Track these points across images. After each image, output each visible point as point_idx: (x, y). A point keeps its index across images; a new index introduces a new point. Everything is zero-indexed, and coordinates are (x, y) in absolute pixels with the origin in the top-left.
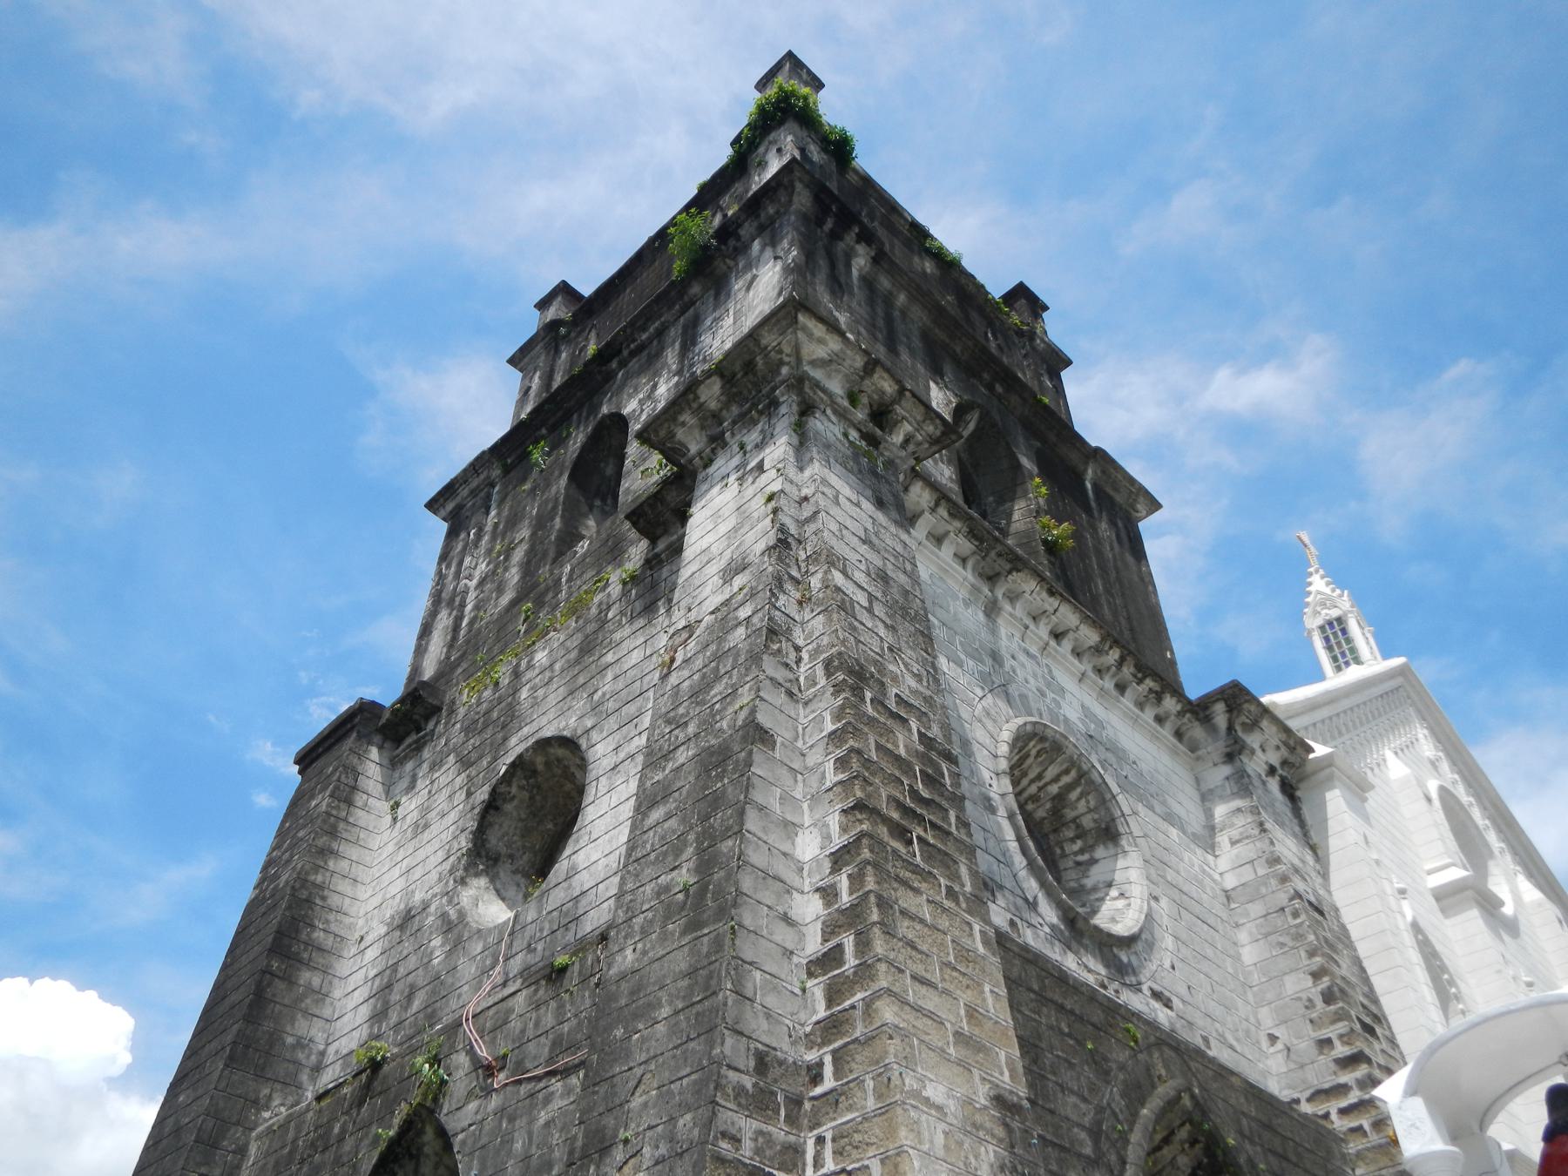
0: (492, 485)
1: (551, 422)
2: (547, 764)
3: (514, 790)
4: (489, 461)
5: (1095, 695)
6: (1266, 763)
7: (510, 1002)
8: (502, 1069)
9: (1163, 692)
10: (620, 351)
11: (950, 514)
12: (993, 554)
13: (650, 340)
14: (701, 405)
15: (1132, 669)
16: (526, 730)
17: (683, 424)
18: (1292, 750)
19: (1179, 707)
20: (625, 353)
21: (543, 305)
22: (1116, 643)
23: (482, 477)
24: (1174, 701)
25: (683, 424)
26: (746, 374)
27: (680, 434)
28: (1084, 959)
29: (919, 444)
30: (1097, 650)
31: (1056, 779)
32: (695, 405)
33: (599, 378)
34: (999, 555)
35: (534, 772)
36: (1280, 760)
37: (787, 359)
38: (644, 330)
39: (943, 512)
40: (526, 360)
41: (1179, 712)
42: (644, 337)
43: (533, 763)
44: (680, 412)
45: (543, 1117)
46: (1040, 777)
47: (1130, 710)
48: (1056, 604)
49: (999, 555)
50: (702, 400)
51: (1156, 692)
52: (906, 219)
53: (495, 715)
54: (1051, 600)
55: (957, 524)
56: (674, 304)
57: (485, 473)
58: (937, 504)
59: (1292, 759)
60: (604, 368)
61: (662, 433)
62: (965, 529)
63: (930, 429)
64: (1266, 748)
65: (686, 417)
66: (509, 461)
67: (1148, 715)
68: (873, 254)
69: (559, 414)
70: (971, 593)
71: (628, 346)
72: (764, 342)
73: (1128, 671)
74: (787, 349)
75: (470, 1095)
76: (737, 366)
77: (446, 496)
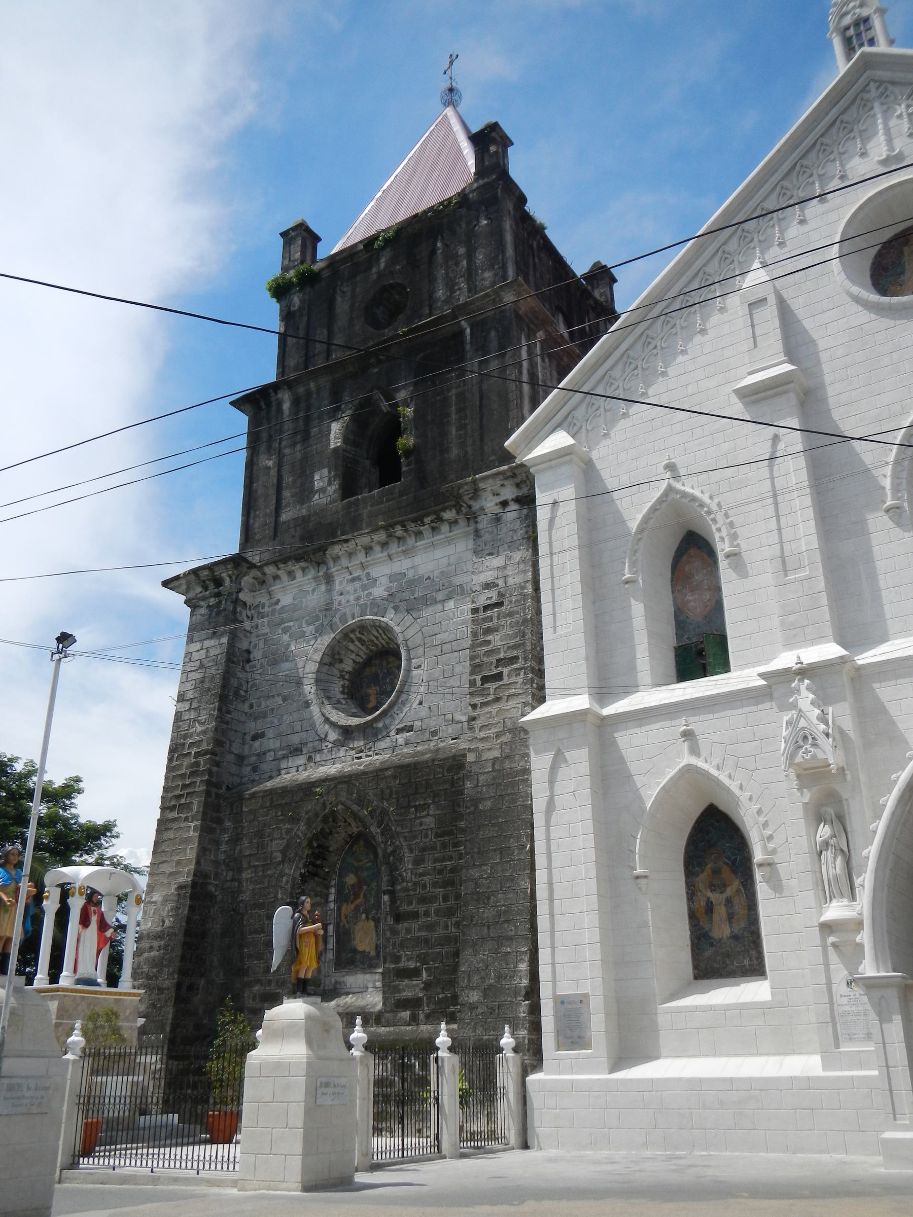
5: (403, 558)
6: (496, 504)
9: (438, 515)
11: (284, 563)
12: (311, 556)
15: (413, 525)
18: (514, 476)
19: (454, 511)
22: (392, 526)
24: (448, 512)
28: (351, 746)
29: (233, 574)
30: (390, 536)
31: (380, 634)
34: (314, 554)
36: (514, 487)
39: (281, 566)
41: (458, 513)
46: (377, 638)
47: (426, 544)
48: (353, 542)
49: (314, 554)
51: (436, 519)
52: (361, 251)
54: (350, 543)
55: (290, 563)
58: (277, 566)
59: (518, 480)
62: (294, 562)
63: (229, 566)
64: (498, 492)
67: (445, 528)
68: (286, 387)
70: (316, 581)
73: (411, 526)
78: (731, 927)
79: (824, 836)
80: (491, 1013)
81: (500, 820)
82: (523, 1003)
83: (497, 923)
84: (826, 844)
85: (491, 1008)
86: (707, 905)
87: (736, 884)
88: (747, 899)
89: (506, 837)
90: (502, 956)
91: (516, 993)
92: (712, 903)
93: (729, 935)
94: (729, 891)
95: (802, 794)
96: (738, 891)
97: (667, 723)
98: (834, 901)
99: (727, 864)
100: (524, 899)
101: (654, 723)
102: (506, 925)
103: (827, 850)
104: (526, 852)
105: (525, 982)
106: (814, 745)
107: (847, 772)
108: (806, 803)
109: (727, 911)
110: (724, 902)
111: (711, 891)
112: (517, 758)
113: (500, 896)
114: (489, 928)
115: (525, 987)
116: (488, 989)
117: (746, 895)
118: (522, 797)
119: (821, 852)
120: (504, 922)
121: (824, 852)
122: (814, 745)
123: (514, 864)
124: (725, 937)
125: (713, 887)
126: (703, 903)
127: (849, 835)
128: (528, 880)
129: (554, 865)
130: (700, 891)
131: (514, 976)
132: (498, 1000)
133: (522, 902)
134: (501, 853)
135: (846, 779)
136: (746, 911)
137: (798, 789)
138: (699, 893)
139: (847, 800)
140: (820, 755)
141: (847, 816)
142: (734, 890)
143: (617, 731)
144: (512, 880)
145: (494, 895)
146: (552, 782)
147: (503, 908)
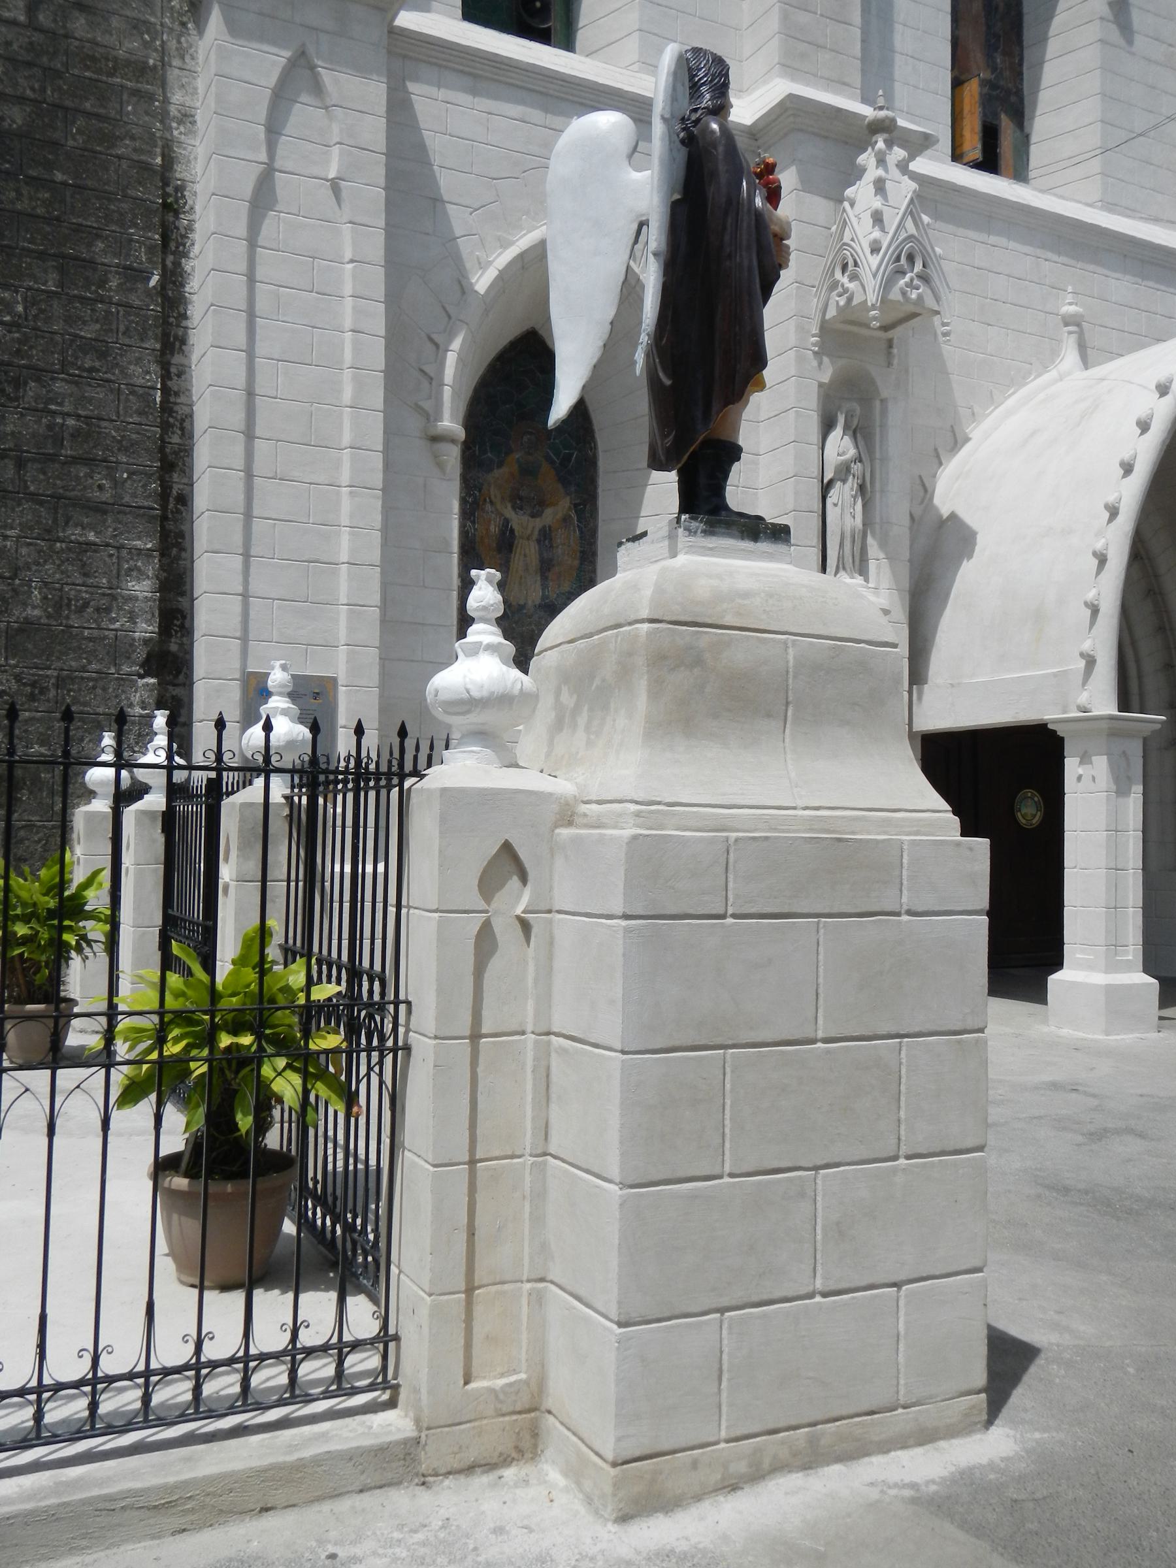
78: (544, 587)
79: (844, 453)
80: (32, 697)
81: (59, 176)
82: (141, 682)
83: (52, 458)
84: (844, 471)
85: (33, 685)
86: (503, 533)
87: (564, 505)
88: (581, 538)
89: (78, 229)
90: (69, 550)
91: (118, 650)
92: (512, 531)
93: (538, 602)
94: (550, 516)
95: (820, 363)
96: (566, 520)
97: (536, 115)
98: (842, 573)
99: (552, 462)
100: (140, 413)
101: (508, 100)
102: (83, 471)
103: (844, 481)
104: (148, 292)
105: (146, 629)
106: (924, 278)
107: (895, 351)
108: (821, 385)
109: (541, 554)
110: (536, 535)
111: (514, 508)
112: (115, 22)
113: (58, 386)
114: (20, 464)
115: (146, 642)
116: (20, 631)
117: (581, 532)
118: (133, 138)
119: (831, 482)
120: (75, 460)
121: (838, 484)
122: (924, 278)
123: (108, 312)
124: (530, 602)
125: (518, 501)
126: (494, 529)
127: (877, 464)
128: (154, 367)
129: (261, 348)
130: (491, 503)
131: (108, 610)
132: (59, 664)
133: (136, 419)
134: (62, 270)
135: (889, 364)
136: (576, 563)
137: (815, 353)
138: (488, 507)
139: (882, 401)
140: (930, 302)
141: (878, 429)
142: (560, 515)
143: (416, 79)
144: (103, 355)
145: (38, 380)
146: (273, 130)
147: (71, 422)
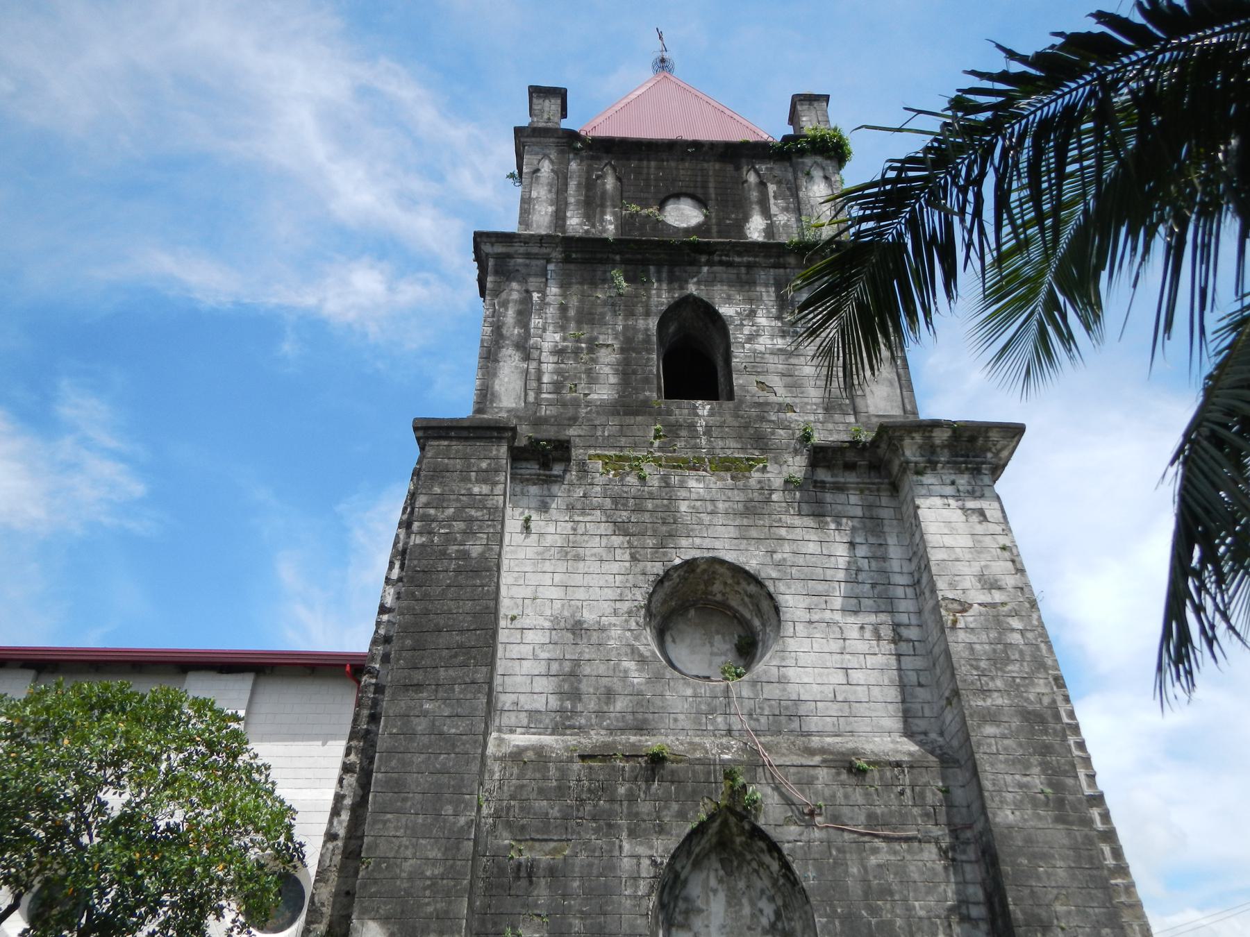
0: (549, 261)
1: (627, 256)
2: (704, 571)
3: (675, 575)
4: (557, 244)
7: (812, 772)
8: (820, 814)
10: (711, 253)
13: (739, 265)
14: (931, 437)
16: (698, 541)
17: (913, 438)
20: (716, 258)
21: (537, 92)
23: (544, 251)
25: (913, 438)
26: (968, 441)
27: (907, 442)
32: (927, 434)
33: (686, 258)
35: (693, 571)
37: (994, 450)
38: (740, 254)
40: (533, 139)
42: (737, 259)
43: (698, 566)
44: (916, 431)
45: (873, 860)
50: (934, 434)
53: (650, 505)
56: (770, 257)
57: (548, 250)
60: (693, 255)
61: (897, 434)
65: (918, 438)
66: (574, 256)
69: (639, 257)
71: (721, 256)
72: (990, 434)
74: (999, 446)
75: (788, 821)
76: (967, 434)
77: (500, 240)
